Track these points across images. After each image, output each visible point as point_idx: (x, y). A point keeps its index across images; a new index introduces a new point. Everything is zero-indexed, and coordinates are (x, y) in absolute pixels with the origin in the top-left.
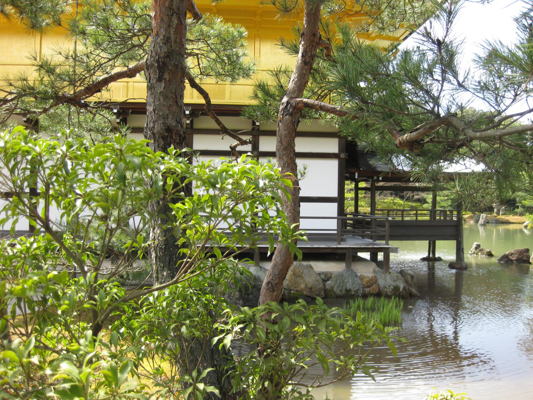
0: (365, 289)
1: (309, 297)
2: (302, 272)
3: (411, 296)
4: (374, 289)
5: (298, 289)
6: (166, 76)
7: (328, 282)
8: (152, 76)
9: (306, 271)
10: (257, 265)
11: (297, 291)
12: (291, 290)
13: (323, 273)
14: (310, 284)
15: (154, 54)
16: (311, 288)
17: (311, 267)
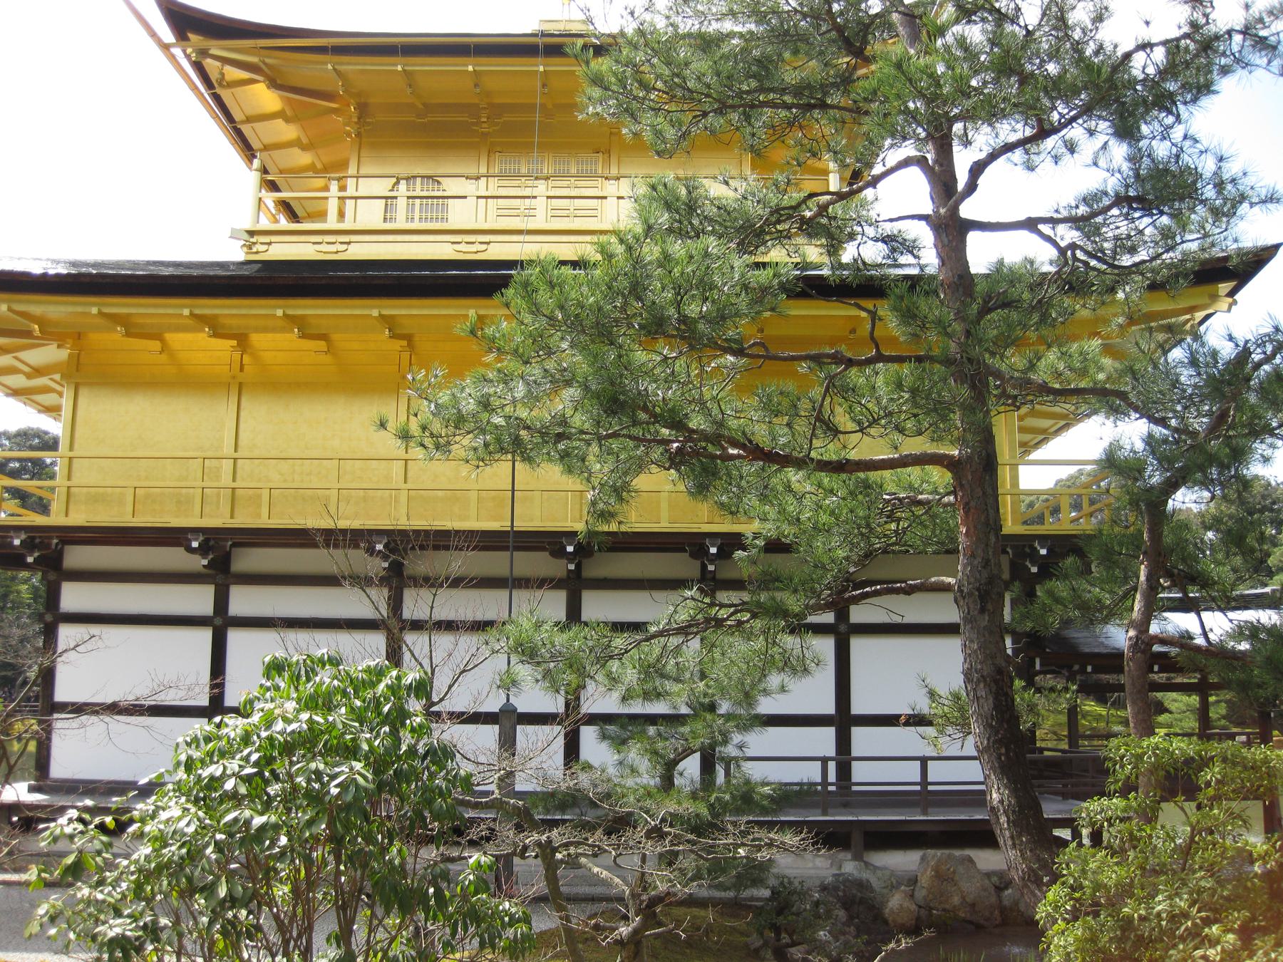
1: (971, 922)
2: (954, 872)
5: (947, 907)
6: (989, 606)
8: (971, 606)
9: (961, 869)
10: (857, 857)
11: (944, 910)
12: (931, 909)
13: (994, 873)
15: (972, 580)
16: (973, 905)
17: (971, 860)
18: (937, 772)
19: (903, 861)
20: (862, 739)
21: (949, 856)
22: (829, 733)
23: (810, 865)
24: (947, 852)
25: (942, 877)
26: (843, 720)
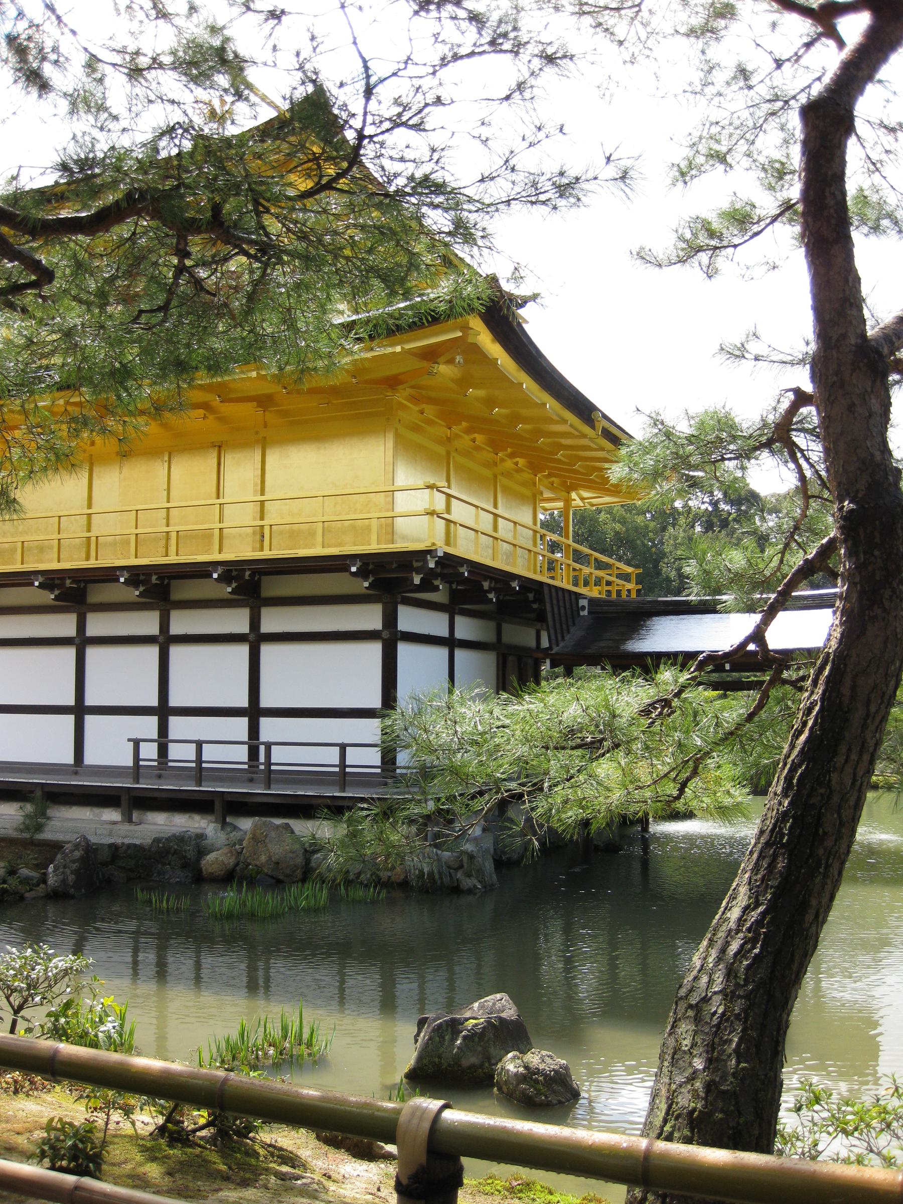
0: (381, 874)
1: (272, 877)
3: (456, 890)
4: (398, 874)
5: (258, 863)
7: (315, 856)
9: (273, 834)
11: (256, 865)
14: (277, 856)
16: (277, 863)
18: (279, 755)
19: (246, 824)
20: (270, 728)
21: (264, 823)
22: (244, 722)
23: (197, 825)
24: (264, 819)
25: (257, 839)
26: (254, 712)
